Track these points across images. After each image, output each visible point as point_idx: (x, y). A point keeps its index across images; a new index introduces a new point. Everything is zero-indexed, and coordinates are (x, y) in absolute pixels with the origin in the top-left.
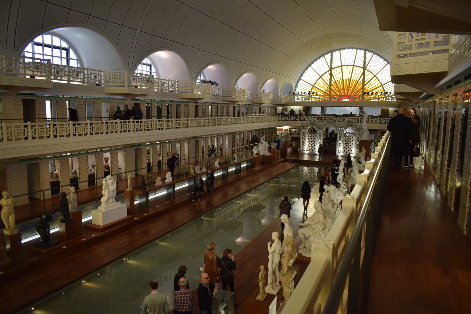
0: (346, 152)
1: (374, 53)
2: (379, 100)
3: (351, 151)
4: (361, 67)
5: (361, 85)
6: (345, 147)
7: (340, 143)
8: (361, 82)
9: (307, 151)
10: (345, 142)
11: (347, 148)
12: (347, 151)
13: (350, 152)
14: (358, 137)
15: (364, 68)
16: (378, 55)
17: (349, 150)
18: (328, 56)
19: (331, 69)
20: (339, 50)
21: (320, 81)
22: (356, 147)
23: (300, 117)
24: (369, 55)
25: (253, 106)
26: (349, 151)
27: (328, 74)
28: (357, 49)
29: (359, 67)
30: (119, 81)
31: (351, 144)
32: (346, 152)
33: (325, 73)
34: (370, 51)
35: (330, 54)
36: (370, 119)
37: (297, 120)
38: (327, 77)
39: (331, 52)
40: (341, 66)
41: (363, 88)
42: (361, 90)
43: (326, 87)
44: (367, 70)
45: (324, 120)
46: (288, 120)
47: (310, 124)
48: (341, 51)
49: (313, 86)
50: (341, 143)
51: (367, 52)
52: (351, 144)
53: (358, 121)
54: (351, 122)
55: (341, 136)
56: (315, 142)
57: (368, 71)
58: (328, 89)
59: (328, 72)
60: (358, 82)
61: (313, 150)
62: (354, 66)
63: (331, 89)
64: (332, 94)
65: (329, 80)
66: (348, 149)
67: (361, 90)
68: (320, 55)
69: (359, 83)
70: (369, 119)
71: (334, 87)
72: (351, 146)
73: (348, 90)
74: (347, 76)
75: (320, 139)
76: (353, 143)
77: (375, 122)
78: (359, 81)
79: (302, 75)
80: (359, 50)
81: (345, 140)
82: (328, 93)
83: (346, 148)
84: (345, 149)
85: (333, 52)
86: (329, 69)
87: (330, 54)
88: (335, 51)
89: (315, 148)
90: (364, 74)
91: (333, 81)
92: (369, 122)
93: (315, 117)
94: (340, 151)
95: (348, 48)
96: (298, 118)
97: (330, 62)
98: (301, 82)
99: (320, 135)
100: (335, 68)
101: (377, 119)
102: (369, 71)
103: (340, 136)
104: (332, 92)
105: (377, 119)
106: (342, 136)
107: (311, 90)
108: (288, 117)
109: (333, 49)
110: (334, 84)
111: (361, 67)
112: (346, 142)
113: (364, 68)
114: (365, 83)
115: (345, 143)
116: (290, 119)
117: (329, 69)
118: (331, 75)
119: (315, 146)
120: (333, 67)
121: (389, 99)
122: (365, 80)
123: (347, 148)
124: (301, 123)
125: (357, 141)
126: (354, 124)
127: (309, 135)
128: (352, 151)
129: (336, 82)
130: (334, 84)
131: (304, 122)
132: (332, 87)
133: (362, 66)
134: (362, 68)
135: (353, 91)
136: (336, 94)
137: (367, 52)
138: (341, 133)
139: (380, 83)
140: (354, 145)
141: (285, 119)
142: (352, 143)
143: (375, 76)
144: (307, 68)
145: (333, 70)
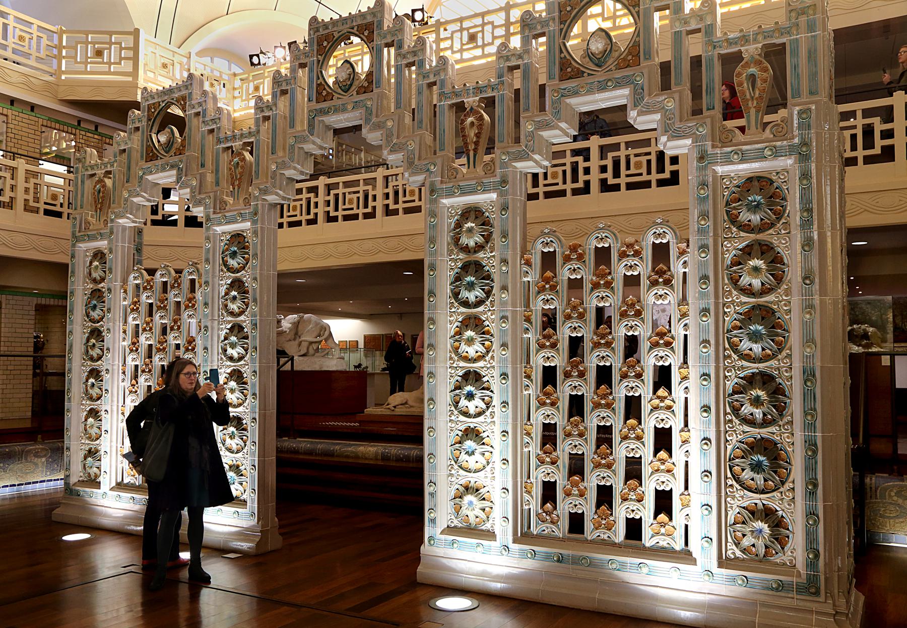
0: (576, 522)
3: (646, 512)
6: (549, 434)
9: (121, 486)
12: (588, 507)
13: (634, 528)
14: (765, 250)
22: (740, 434)
26: (621, 512)
32: (576, 522)
81: (550, 321)
83: (565, 448)
94: (472, 508)
112: (559, 360)
115: (549, 375)
138: (473, 213)
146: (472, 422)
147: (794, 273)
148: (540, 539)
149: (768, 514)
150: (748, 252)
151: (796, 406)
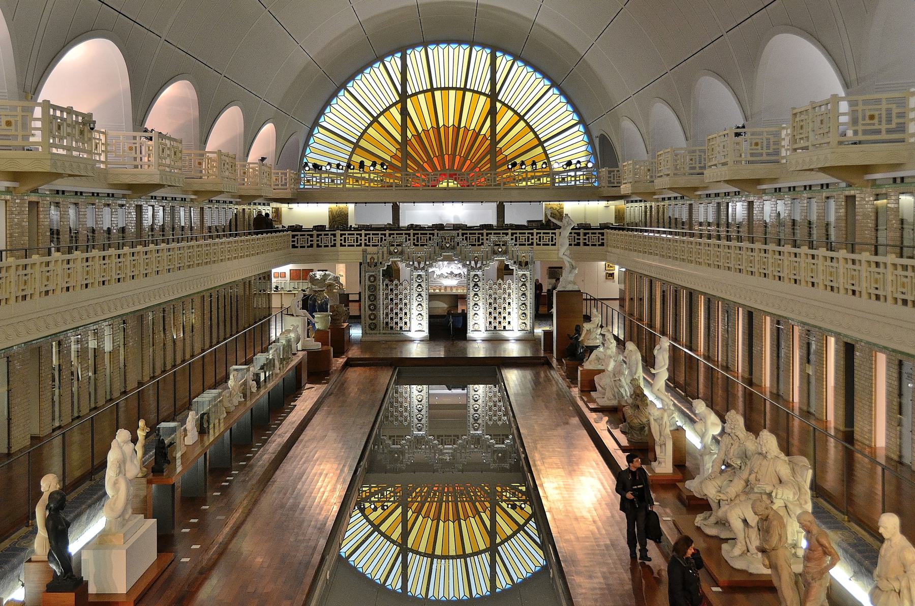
0: (495, 327)
1: (516, 57)
2: (578, 183)
3: (506, 324)
4: (484, 94)
5: (488, 142)
6: (490, 313)
7: (477, 304)
8: (488, 135)
10: (489, 301)
11: (497, 315)
12: (497, 325)
13: (504, 327)
15: (493, 96)
17: (502, 320)
18: (394, 63)
19: (404, 96)
20: (425, 44)
22: (521, 312)
23: (341, 235)
24: (504, 61)
25: (175, 204)
26: (503, 325)
28: (472, 44)
30: (765, 151)
31: (506, 306)
32: (495, 327)
33: (388, 109)
34: (505, 52)
35: (399, 55)
36: (537, 233)
37: (334, 245)
42: (488, 157)
44: (500, 101)
45: (485, 241)
46: (311, 246)
47: (390, 253)
49: (356, 145)
50: (480, 304)
51: (498, 54)
52: (506, 306)
53: (531, 241)
54: (503, 245)
55: (477, 285)
56: (406, 304)
57: (503, 103)
58: (399, 154)
59: (397, 103)
61: (401, 328)
65: (399, 129)
66: (498, 320)
67: (488, 157)
68: (373, 57)
69: (480, 138)
70: (535, 234)
72: (507, 310)
73: (454, 155)
75: (420, 295)
76: (511, 301)
77: (550, 243)
78: (483, 132)
79: (322, 113)
82: (400, 165)
83: (493, 315)
84: (492, 320)
85: (409, 52)
86: (398, 99)
87: (399, 55)
88: (413, 46)
89: (406, 323)
90: (492, 113)
92: (535, 241)
93: (460, 232)
94: (476, 327)
96: (338, 237)
97: (399, 77)
98: (319, 133)
99: (420, 285)
101: (555, 233)
102: (507, 105)
103: (476, 285)
105: (555, 233)
106: (480, 284)
107: (351, 156)
108: (311, 236)
110: (413, 140)
111: (484, 94)
114: (498, 138)
115: (490, 304)
116: (315, 243)
117: (398, 99)
118: (404, 113)
119: (408, 316)
120: (410, 93)
121: (573, 179)
122: (498, 128)
123: (497, 315)
124: (364, 251)
125: (524, 294)
126: (511, 249)
127: (387, 285)
128: (509, 323)
130: (413, 140)
131: (370, 249)
132: (408, 148)
135: (466, 159)
137: (498, 54)
138: (477, 275)
140: (514, 305)
141: (351, 240)
142: (507, 301)
144: (335, 95)
145: (409, 100)
146: (476, 312)
147: (529, 288)
148: (489, 331)
149: (524, 323)
150: (522, 285)
151: (529, 307)
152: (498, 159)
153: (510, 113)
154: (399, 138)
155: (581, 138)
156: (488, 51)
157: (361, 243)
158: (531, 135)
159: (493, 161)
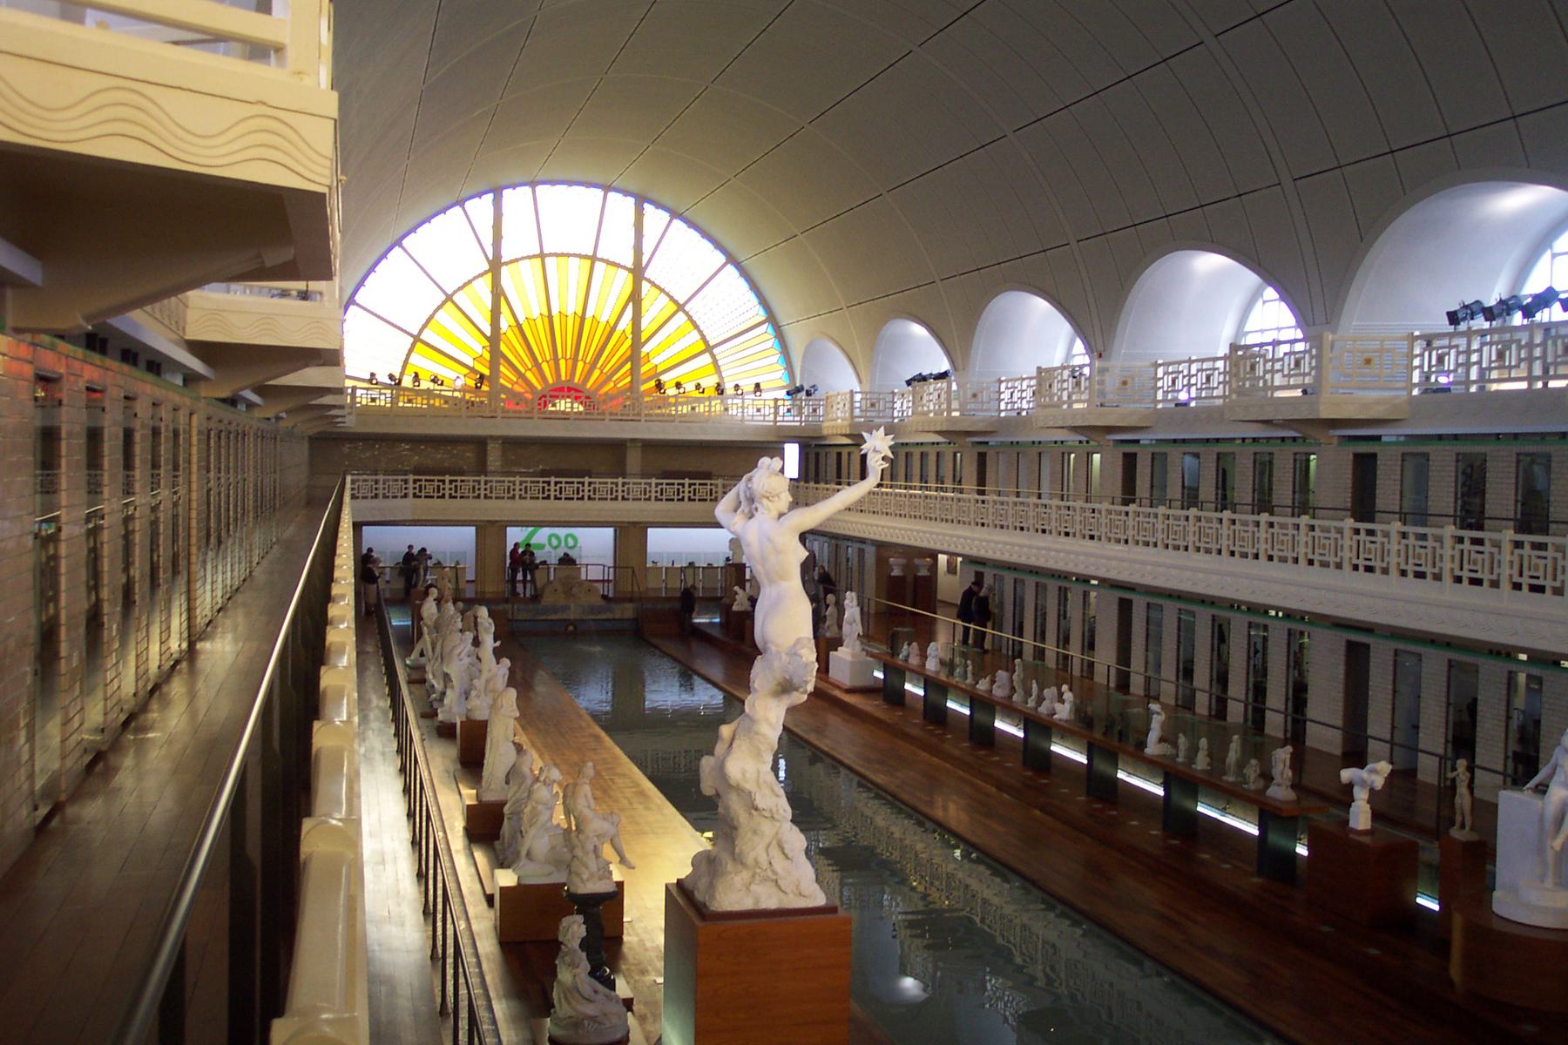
1: (675, 214)
4: (624, 267)
5: (629, 342)
15: (638, 272)
16: (691, 224)
18: (481, 207)
19: (495, 265)
20: (533, 184)
21: (447, 316)
27: (484, 286)
29: (618, 266)
34: (658, 205)
38: (478, 300)
39: (497, 192)
40: (542, 256)
41: (635, 357)
42: (628, 366)
43: (479, 346)
44: (649, 281)
48: (539, 189)
57: (653, 284)
58: (487, 356)
59: (485, 273)
60: (613, 329)
62: (593, 259)
63: (496, 355)
64: (509, 380)
67: (628, 366)
71: (511, 346)
74: (567, 303)
79: (361, 284)
80: (612, 196)
82: (486, 372)
85: (507, 193)
86: (487, 267)
90: (635, 298)
91: (506, 321)
95: (570, 183)
100: (517, 260)
102: (658, 287)
104: (502, 369)
109: (504, 183)
110: (510, 335)
111: (624, 267)
113: (638, 272)
114: (644, 338)
118: (498, 293)
122: (644, 323)
129: (519, 326)
130: (510, 335)
132: (503, 348)
133: (630, 264)
134: (629, 270)
136: (521, 376)
139: (703, 338)
143: (681, 307)
145: (504, 270)
152: (644, 369)
153: (664, 299)
154: (488, 333)
155: (770, 344)
156: (631, 200)
157: (444, 495)
158: (695, 336)
159: (634, 371)
